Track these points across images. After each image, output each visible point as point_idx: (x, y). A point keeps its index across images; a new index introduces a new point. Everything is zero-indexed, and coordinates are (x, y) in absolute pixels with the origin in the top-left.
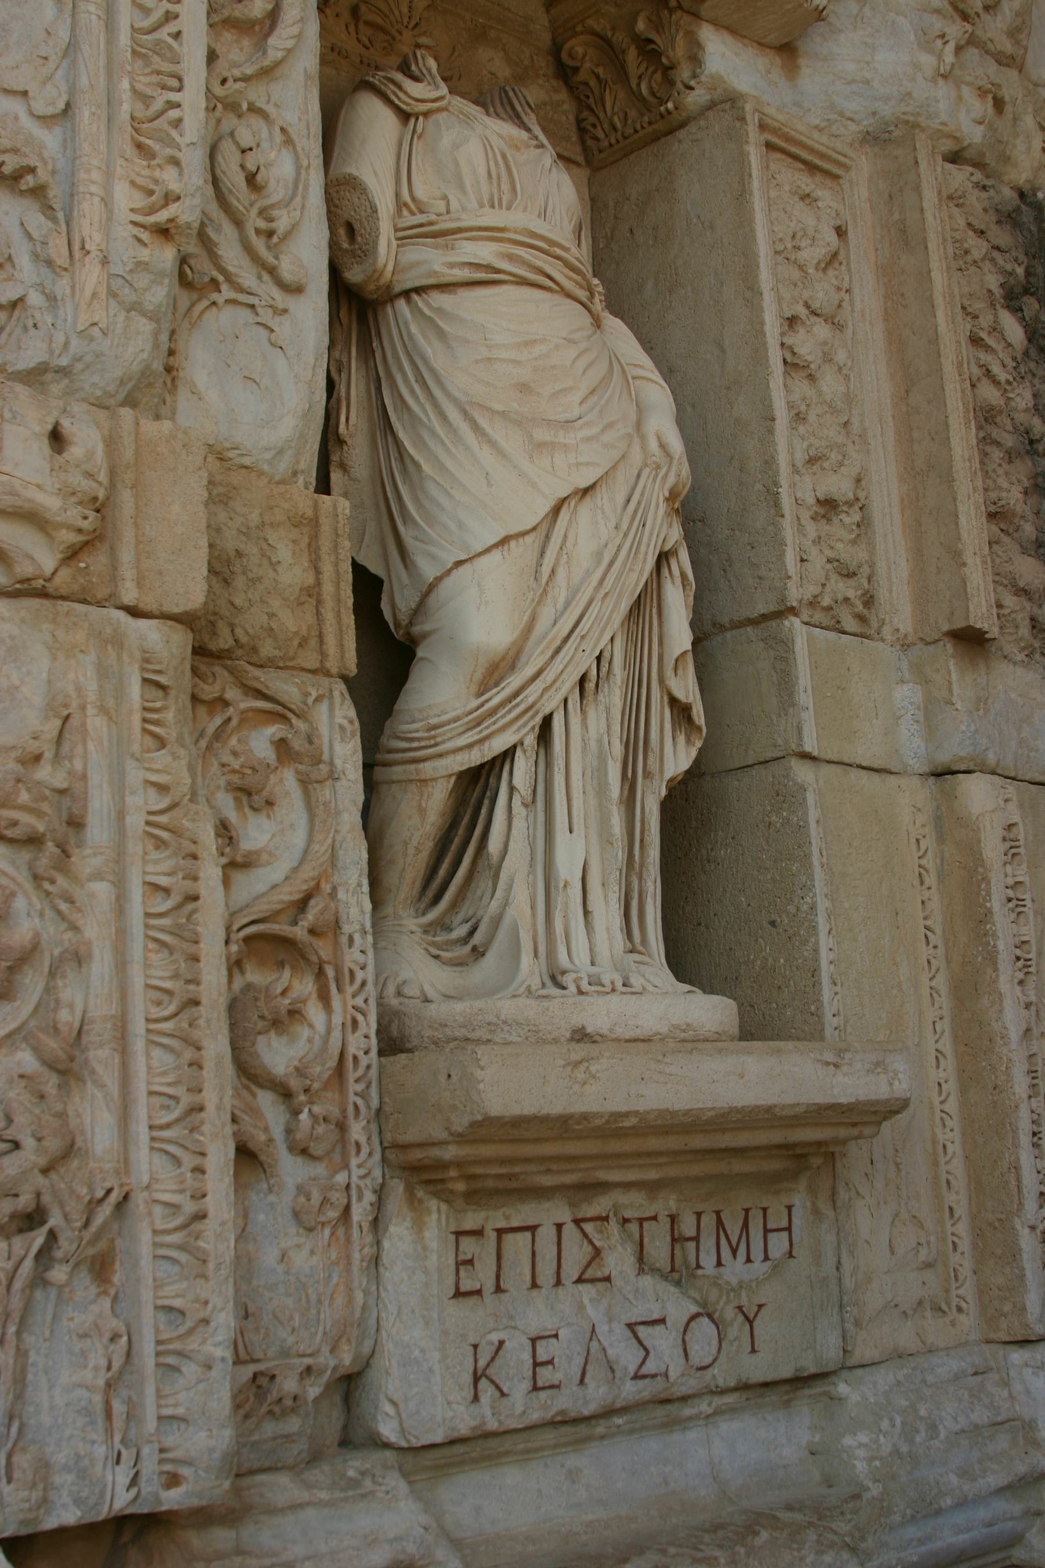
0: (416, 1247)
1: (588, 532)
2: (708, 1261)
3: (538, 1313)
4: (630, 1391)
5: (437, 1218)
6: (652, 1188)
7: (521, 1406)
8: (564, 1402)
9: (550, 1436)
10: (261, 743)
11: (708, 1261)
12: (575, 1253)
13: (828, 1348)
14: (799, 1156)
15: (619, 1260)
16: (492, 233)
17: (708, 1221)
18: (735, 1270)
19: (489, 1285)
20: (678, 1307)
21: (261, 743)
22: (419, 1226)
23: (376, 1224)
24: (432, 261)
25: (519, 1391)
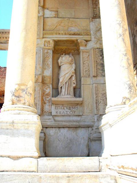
0: (53, 107)
1: (67, 75)
2: (72, 109)
3: (60, 110)
4: (66, 114)
5: (54, 106)
6: (68, 105)
7: (59, 114)
8: (62, 114)
9: (61, 116)
10: (47, 87)
11: (72, 109)
12: (62, 108)
13: (81, 114)
14: (81, 104)
15: (65, 108)
16: (63, 62)
17: (72, 107)
18: (73, 109)
19: (57, 109)
20: (69, 111)
21: (47, 87)
22: (53, 106)
23: (52, 106)
24: (61, 64)
25: (59, 114)
